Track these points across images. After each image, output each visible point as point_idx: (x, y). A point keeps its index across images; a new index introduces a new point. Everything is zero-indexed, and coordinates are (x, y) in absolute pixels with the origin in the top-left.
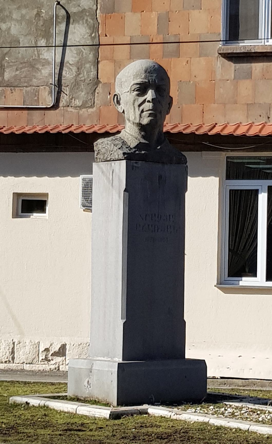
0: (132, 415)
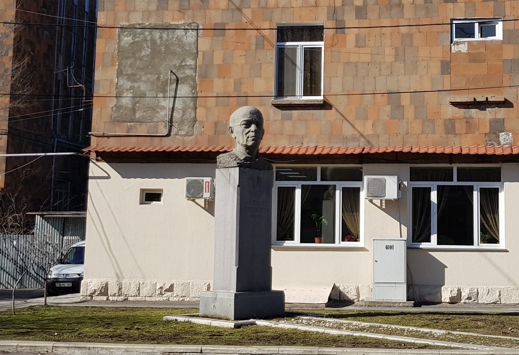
0: (247, 326)
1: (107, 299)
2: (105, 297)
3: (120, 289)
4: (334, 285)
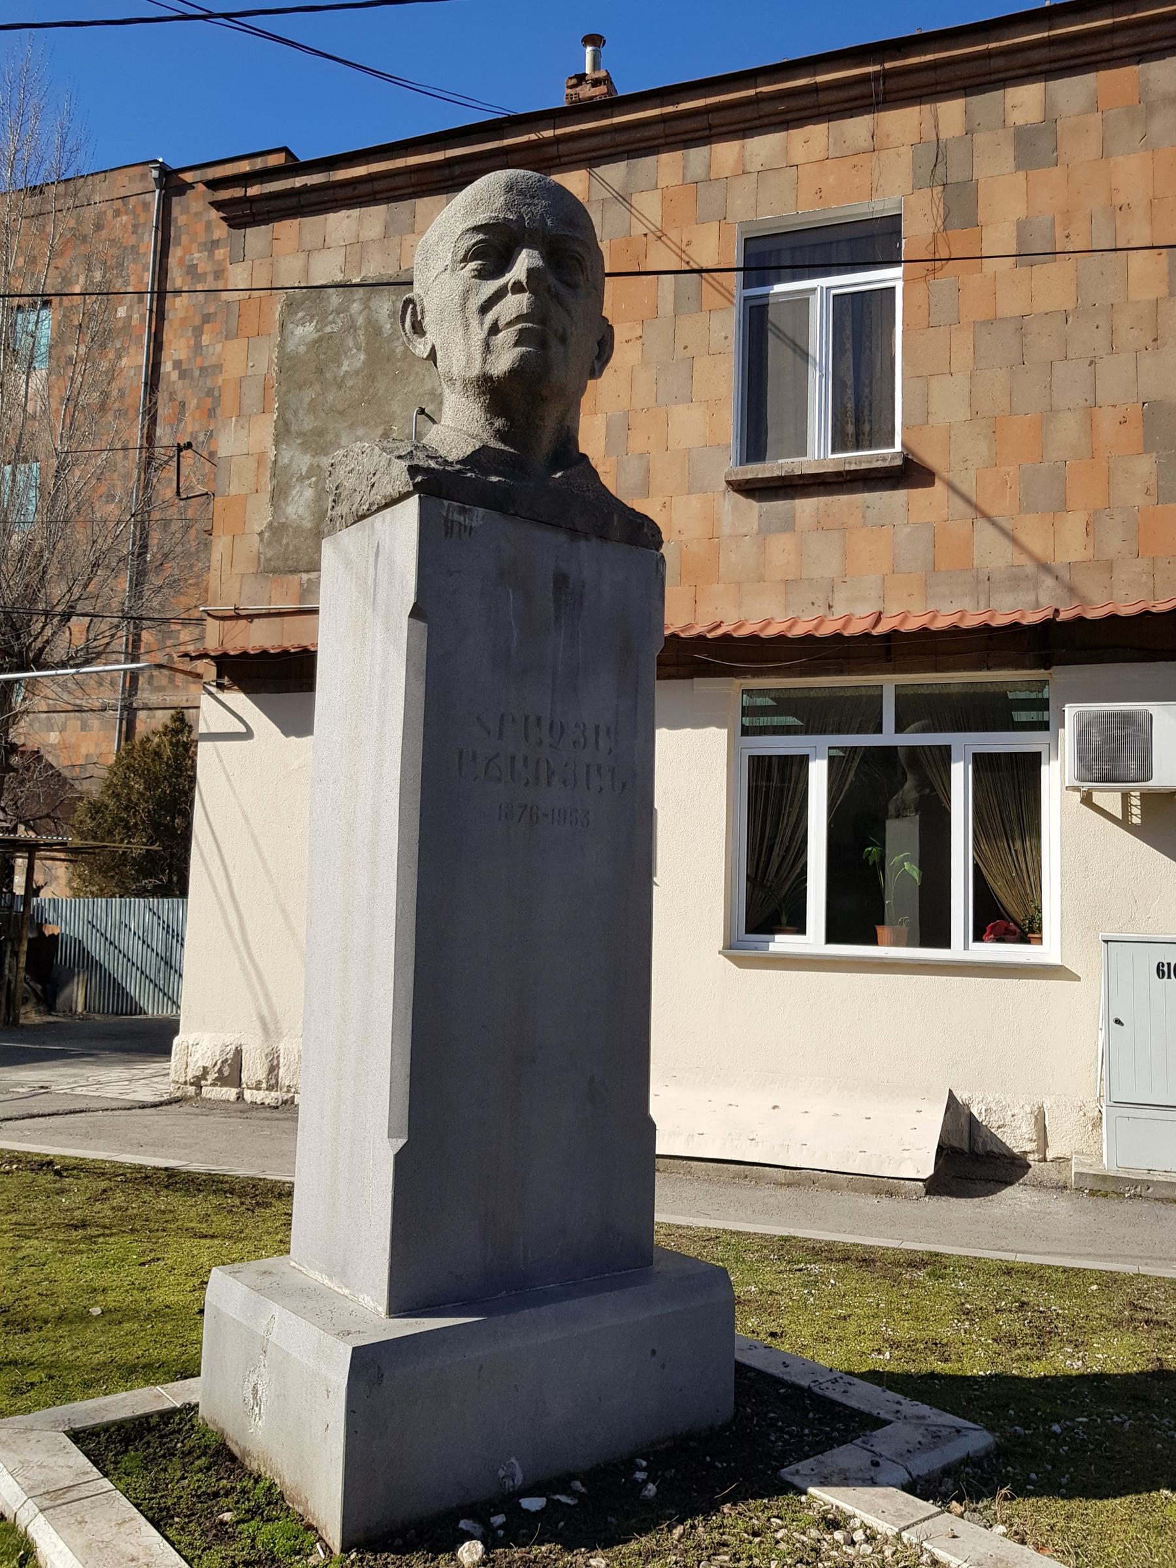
1: (238, 1098)
2: (233, 1089)
3: (273, 1069)
4: (951, 1096)
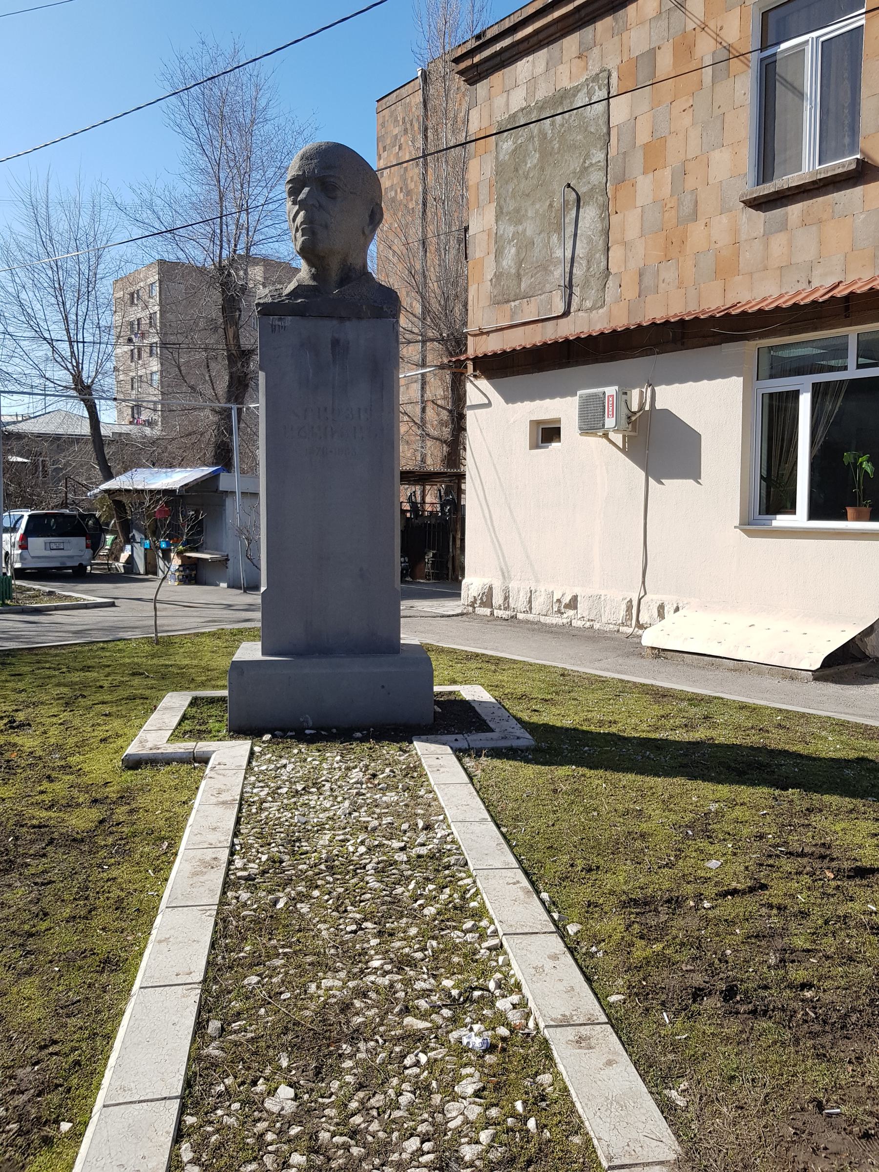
3: (506, 598)
